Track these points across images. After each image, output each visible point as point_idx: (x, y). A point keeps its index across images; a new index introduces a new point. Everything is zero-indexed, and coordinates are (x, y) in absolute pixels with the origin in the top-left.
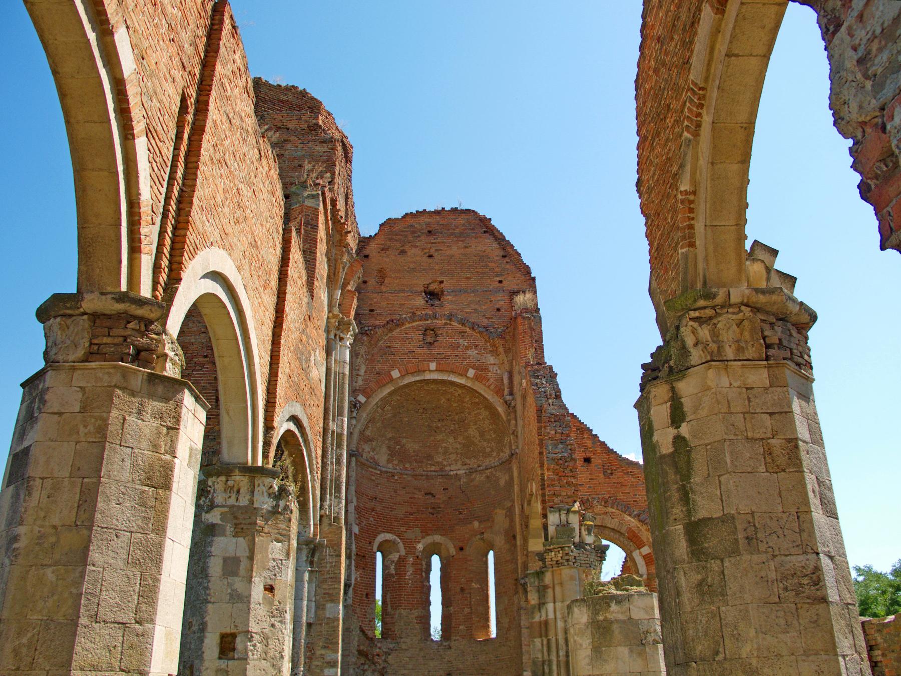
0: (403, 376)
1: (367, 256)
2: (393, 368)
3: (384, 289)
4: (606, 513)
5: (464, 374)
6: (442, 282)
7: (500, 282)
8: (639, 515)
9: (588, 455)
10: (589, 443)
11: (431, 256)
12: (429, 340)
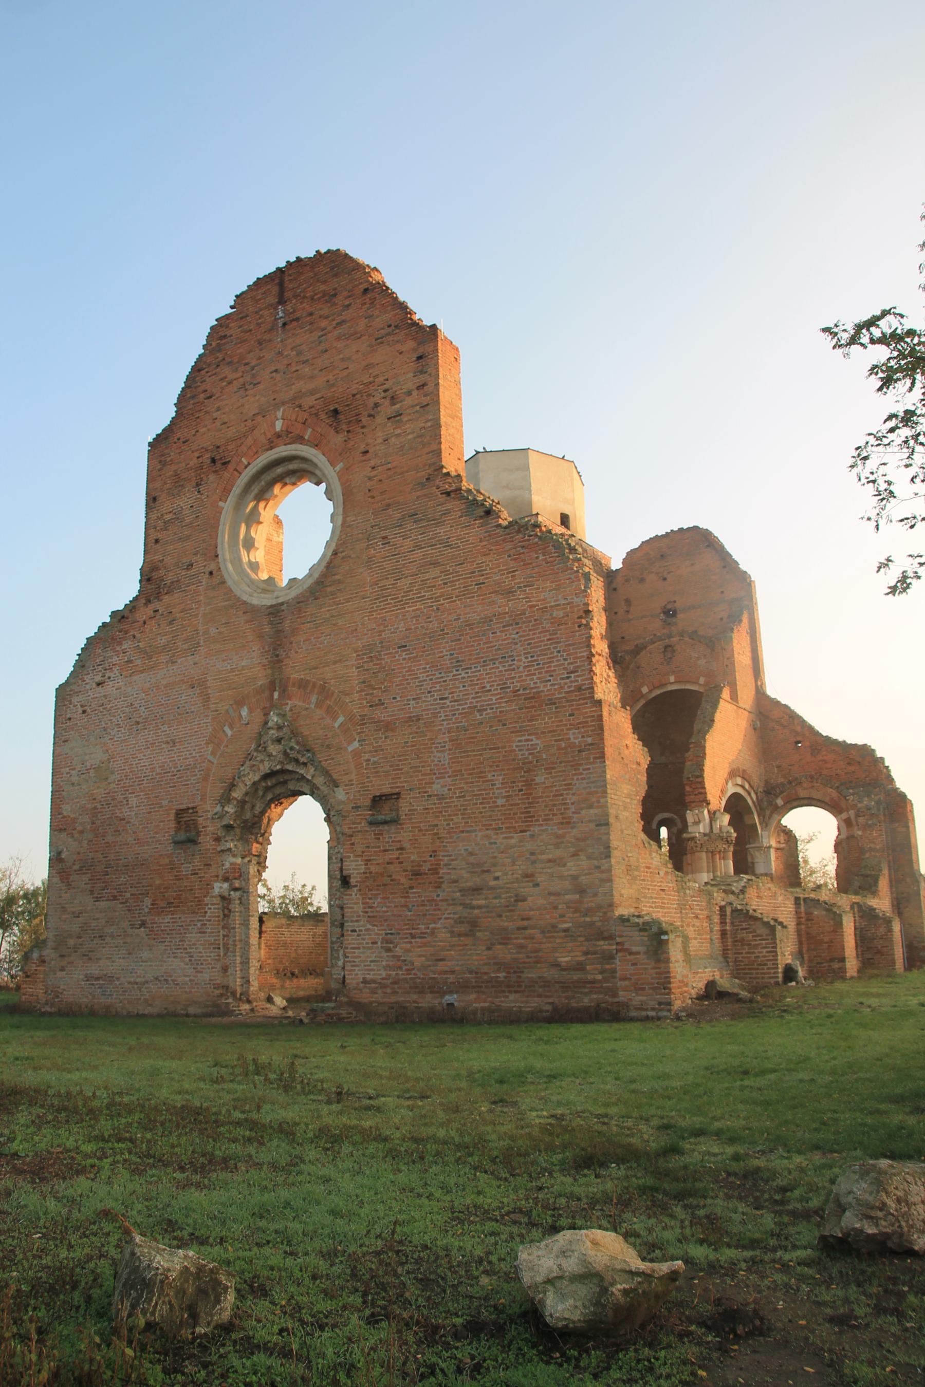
0: (650, 691)
1: (615, 589)
2: (642, 685)
3: (630, 617)
4: (813, 787)
5: (697, 683)
6: (675, 602)
7: (722, 592)
8: (838, 787)
9: (799, 739)
10: (799, 729)
11: (665, 579)
12: (670, 655)
